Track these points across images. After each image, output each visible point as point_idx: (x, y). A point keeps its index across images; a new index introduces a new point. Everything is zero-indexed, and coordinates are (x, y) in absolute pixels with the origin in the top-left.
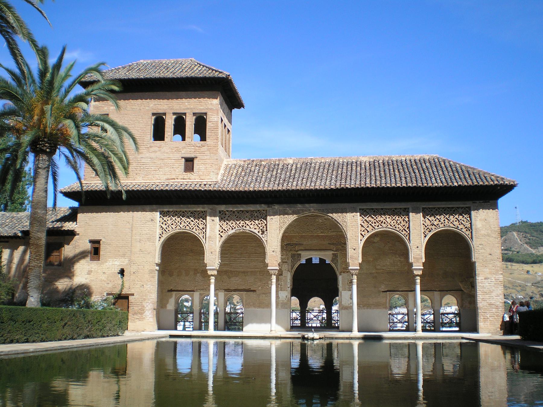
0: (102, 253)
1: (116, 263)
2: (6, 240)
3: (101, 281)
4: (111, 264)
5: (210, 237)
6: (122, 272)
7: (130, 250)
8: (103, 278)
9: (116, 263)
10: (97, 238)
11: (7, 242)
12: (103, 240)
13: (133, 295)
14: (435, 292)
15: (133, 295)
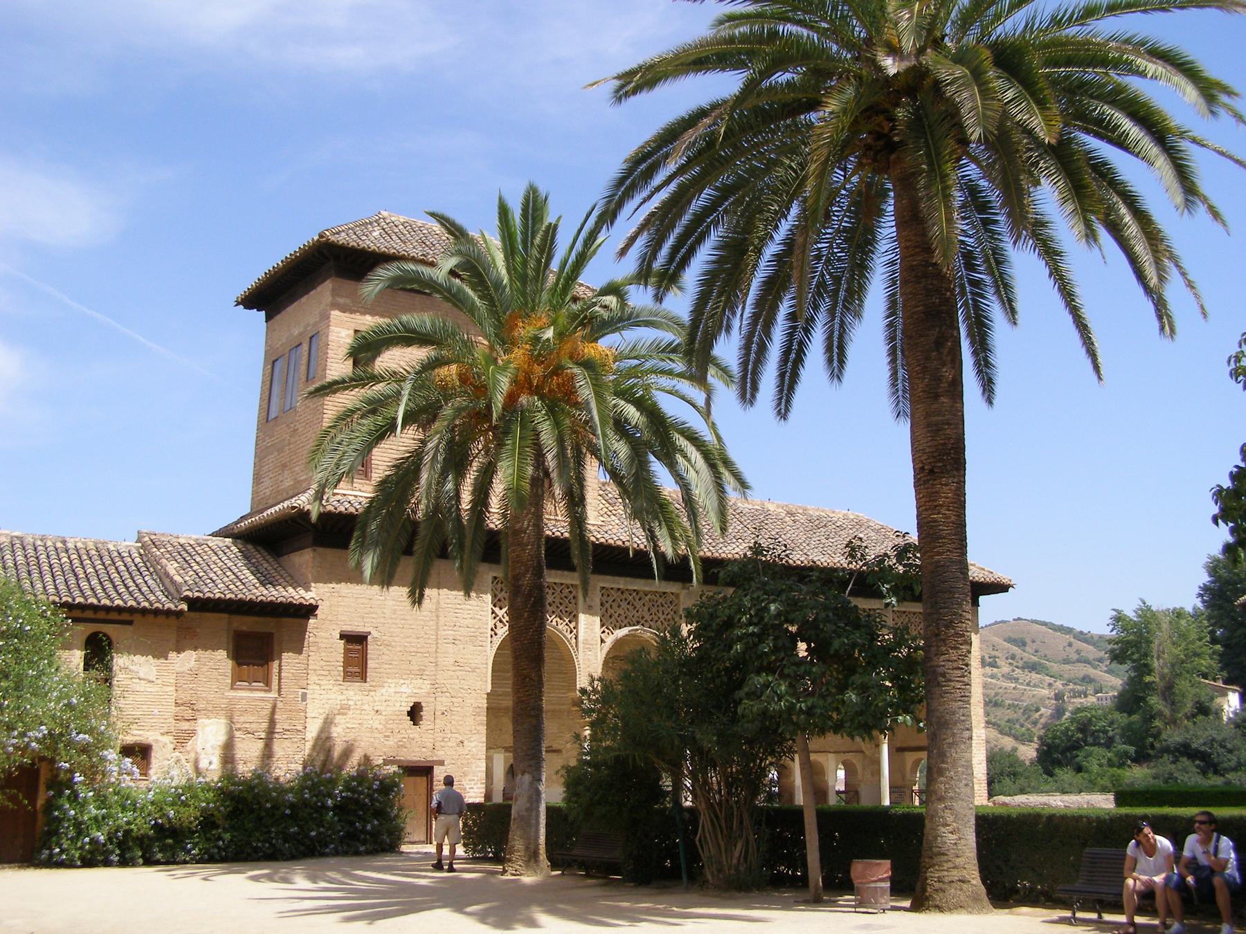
0: (371, 664)
1: (404, 689)
2: (125, 617)
3: (371, 730)
4: (392, 690)
5: (586, 642)
6: (415, 713)
7: (432, 660)
8: (376, 725)
9: (404, 689)
10: (357, 627)
11: (130, 623)
12: (375, 633)
13: (441, 763)
14: (830, 755)
15: (441, 763)
